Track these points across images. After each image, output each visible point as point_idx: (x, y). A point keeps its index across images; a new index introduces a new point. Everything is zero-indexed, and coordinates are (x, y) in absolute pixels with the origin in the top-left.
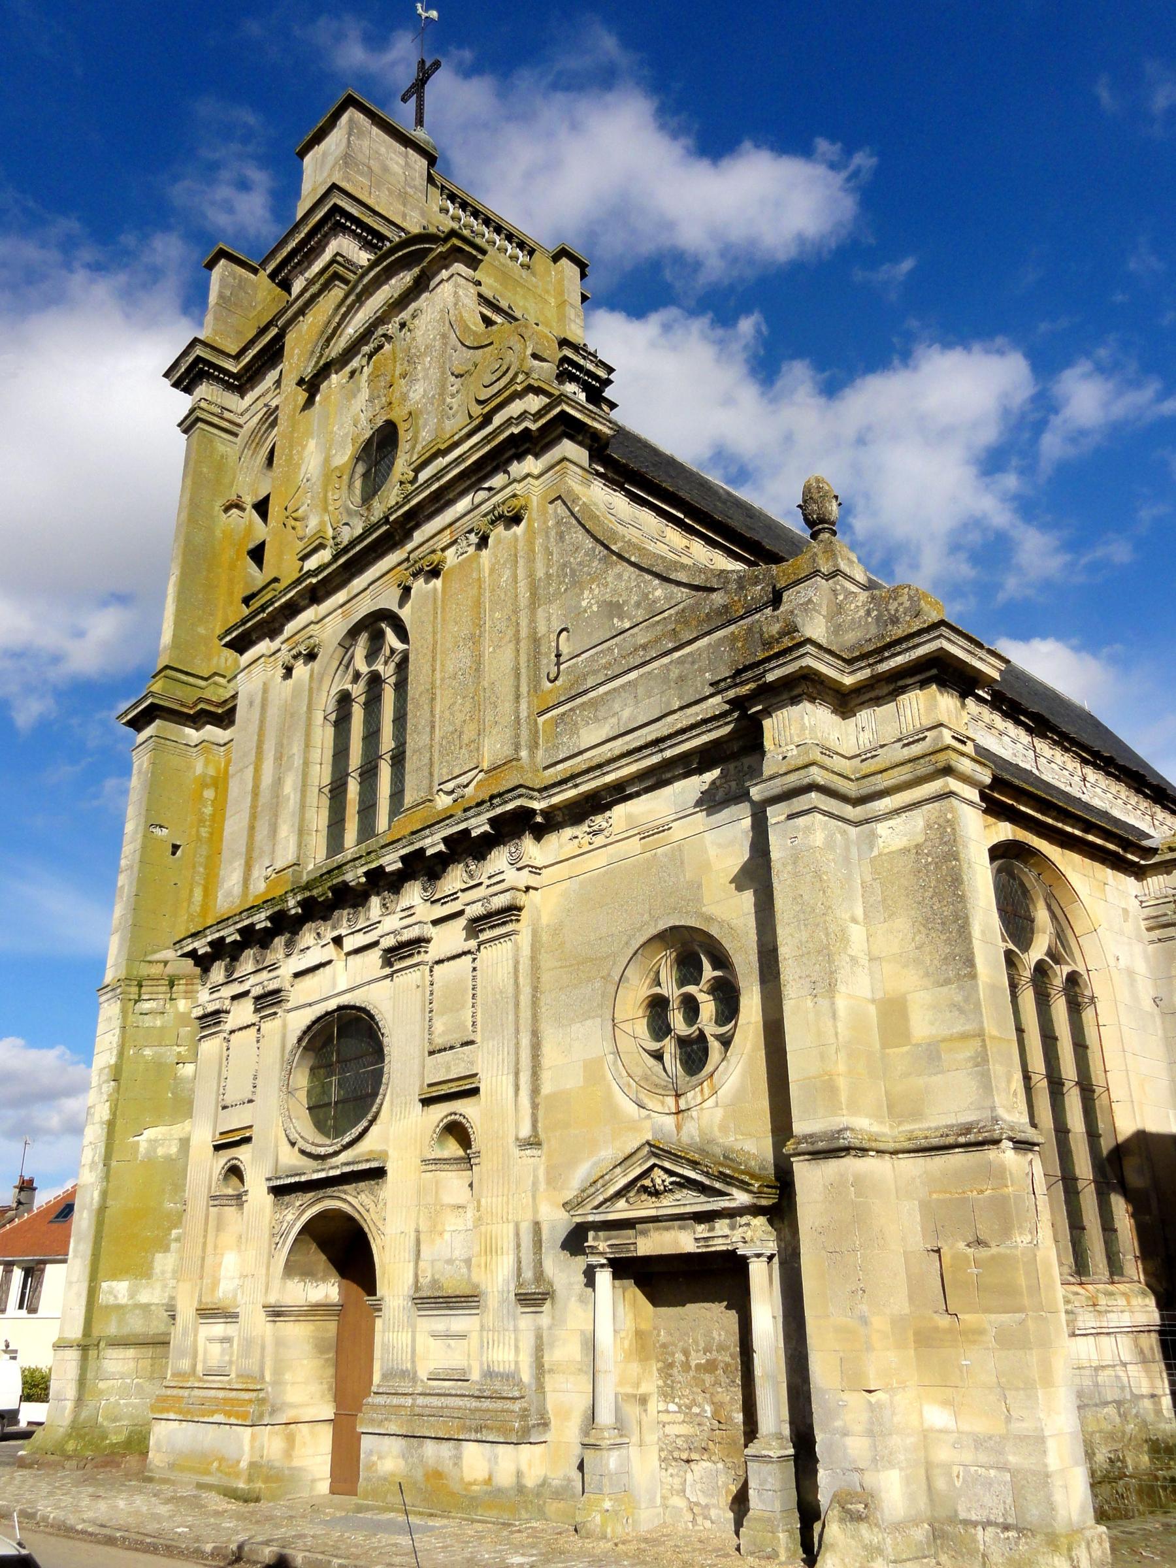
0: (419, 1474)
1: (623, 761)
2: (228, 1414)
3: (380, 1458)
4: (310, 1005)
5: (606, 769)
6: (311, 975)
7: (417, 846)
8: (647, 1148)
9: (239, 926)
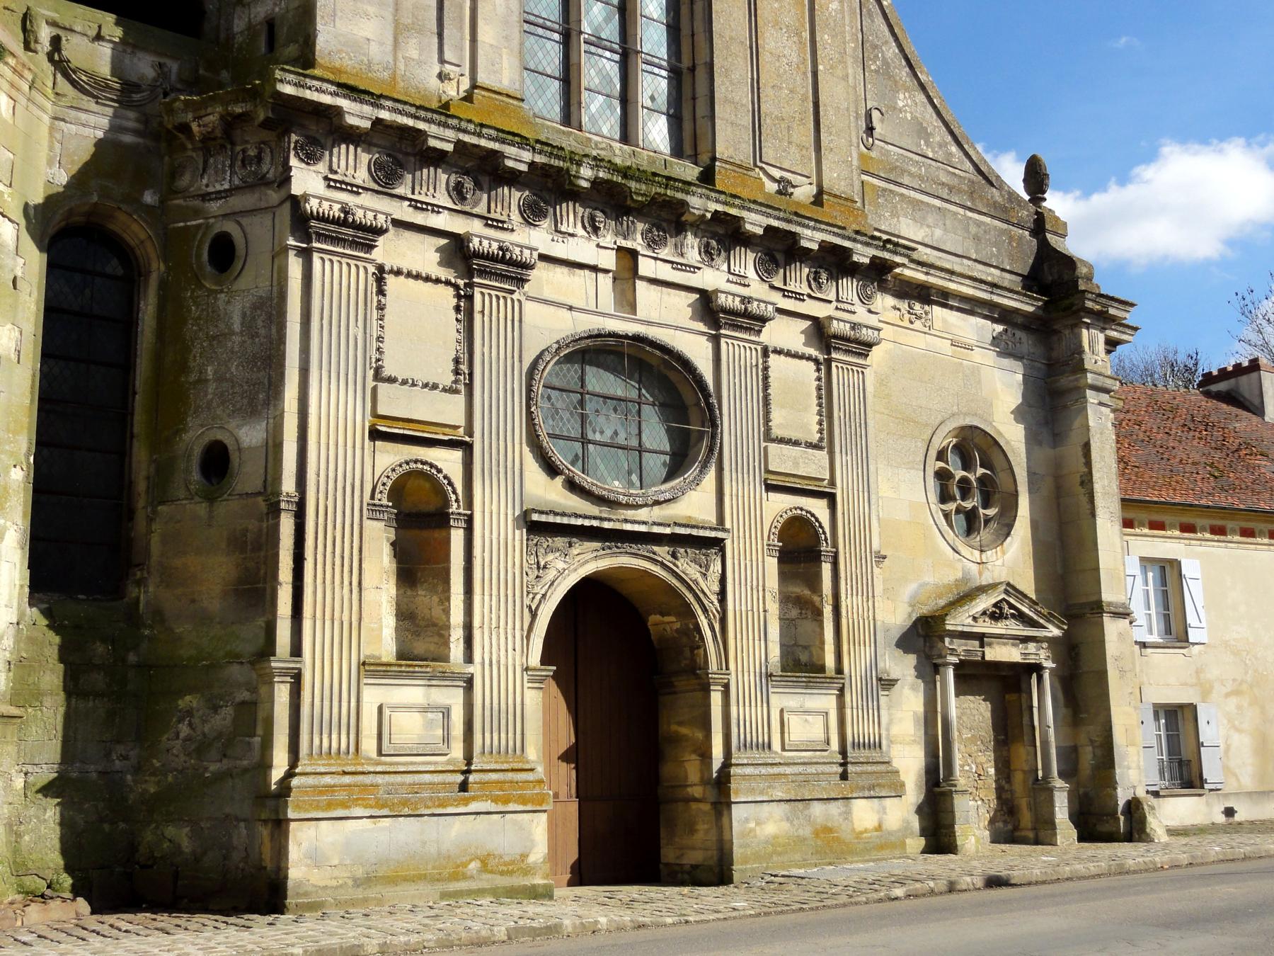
0: (806, 832)
1: (968, 282)
2: (495, 800)
3: (758, 824)
4: (571, 308)
5: (954, 278)
6: (565, 270)
7: (793, 228)
8: (1004, 587)
9: (467, 138)
